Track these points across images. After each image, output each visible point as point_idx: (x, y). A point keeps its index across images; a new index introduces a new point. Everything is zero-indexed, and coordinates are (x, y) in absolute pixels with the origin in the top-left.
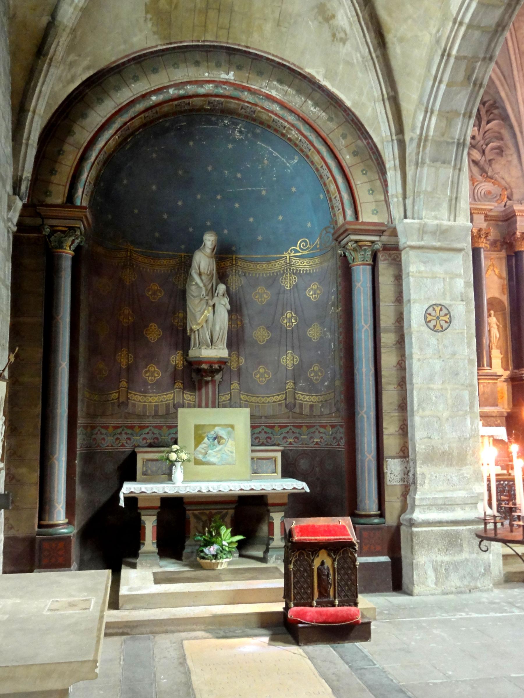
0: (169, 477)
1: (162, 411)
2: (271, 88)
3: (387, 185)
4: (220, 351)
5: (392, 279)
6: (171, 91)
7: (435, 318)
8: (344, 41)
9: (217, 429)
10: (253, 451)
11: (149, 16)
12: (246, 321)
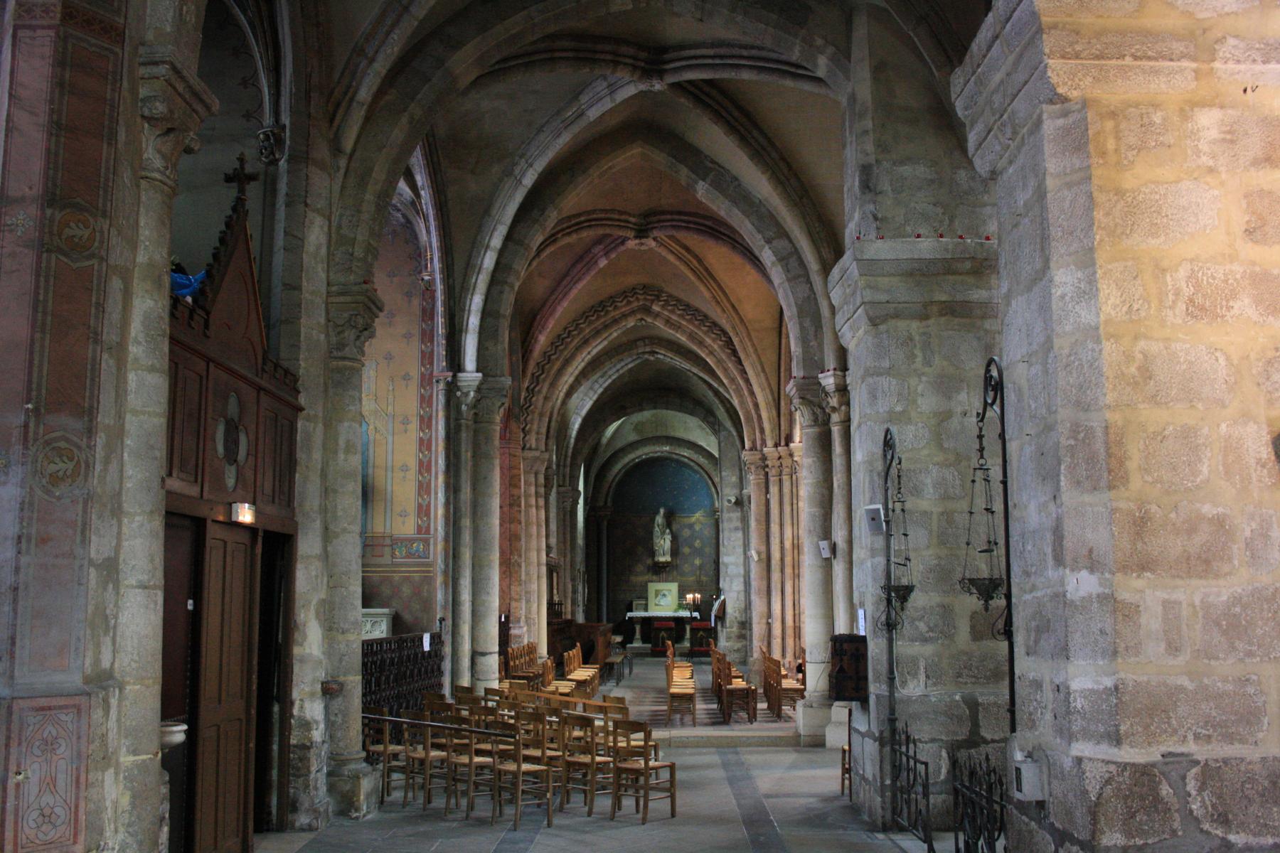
0: (646, 610)
4: (669, 559)
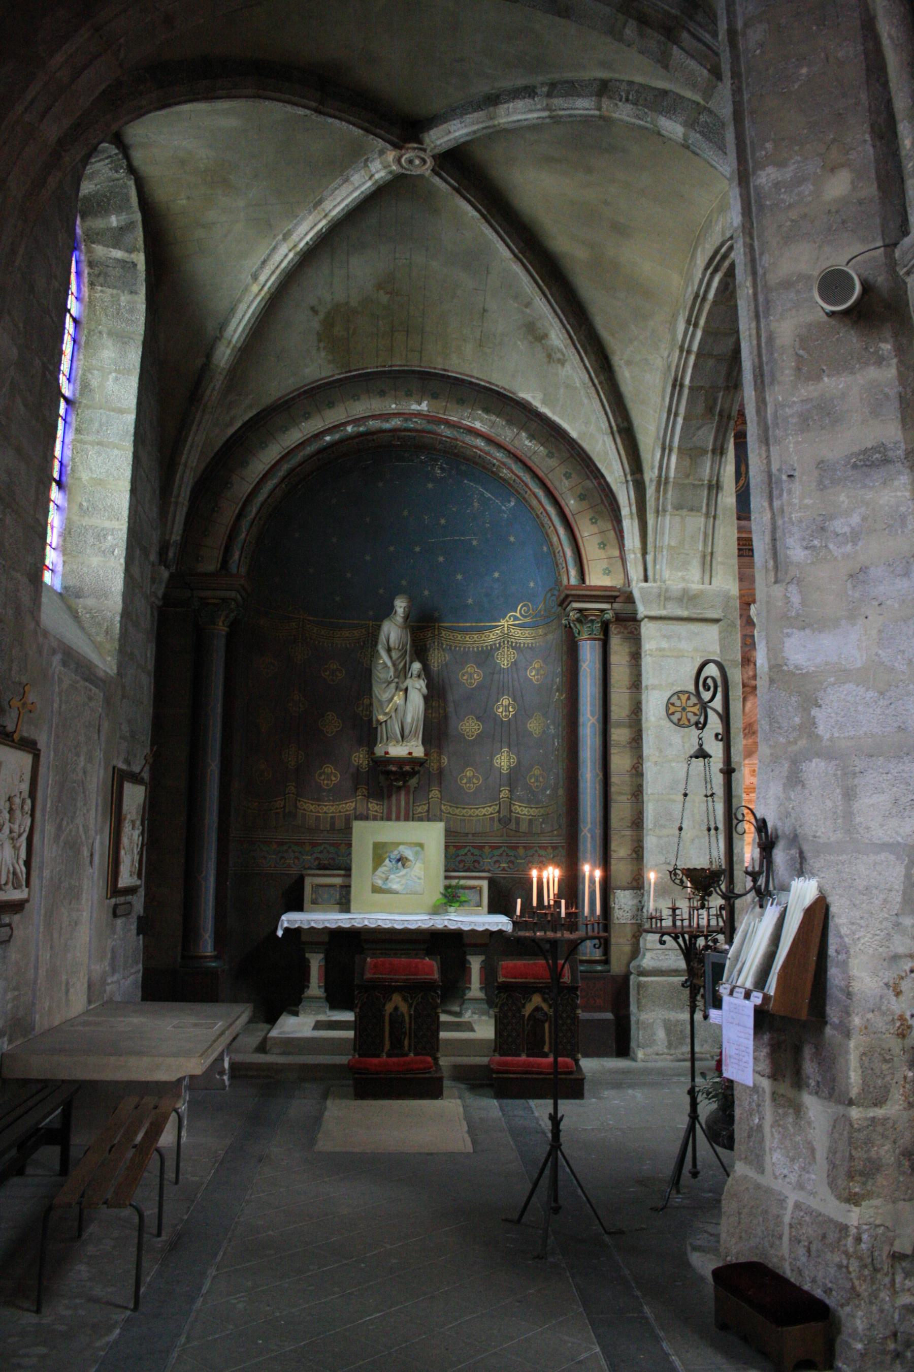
1: (339, 824)
2: (474, 419)
3: (622, 537)
5: (627, 658)
6: (349, 429)
7: (679, 709)
8: (562, 362)
9: (401, 848)
10: (446, 878)
11: (322, 345)
12: (451, 709)
